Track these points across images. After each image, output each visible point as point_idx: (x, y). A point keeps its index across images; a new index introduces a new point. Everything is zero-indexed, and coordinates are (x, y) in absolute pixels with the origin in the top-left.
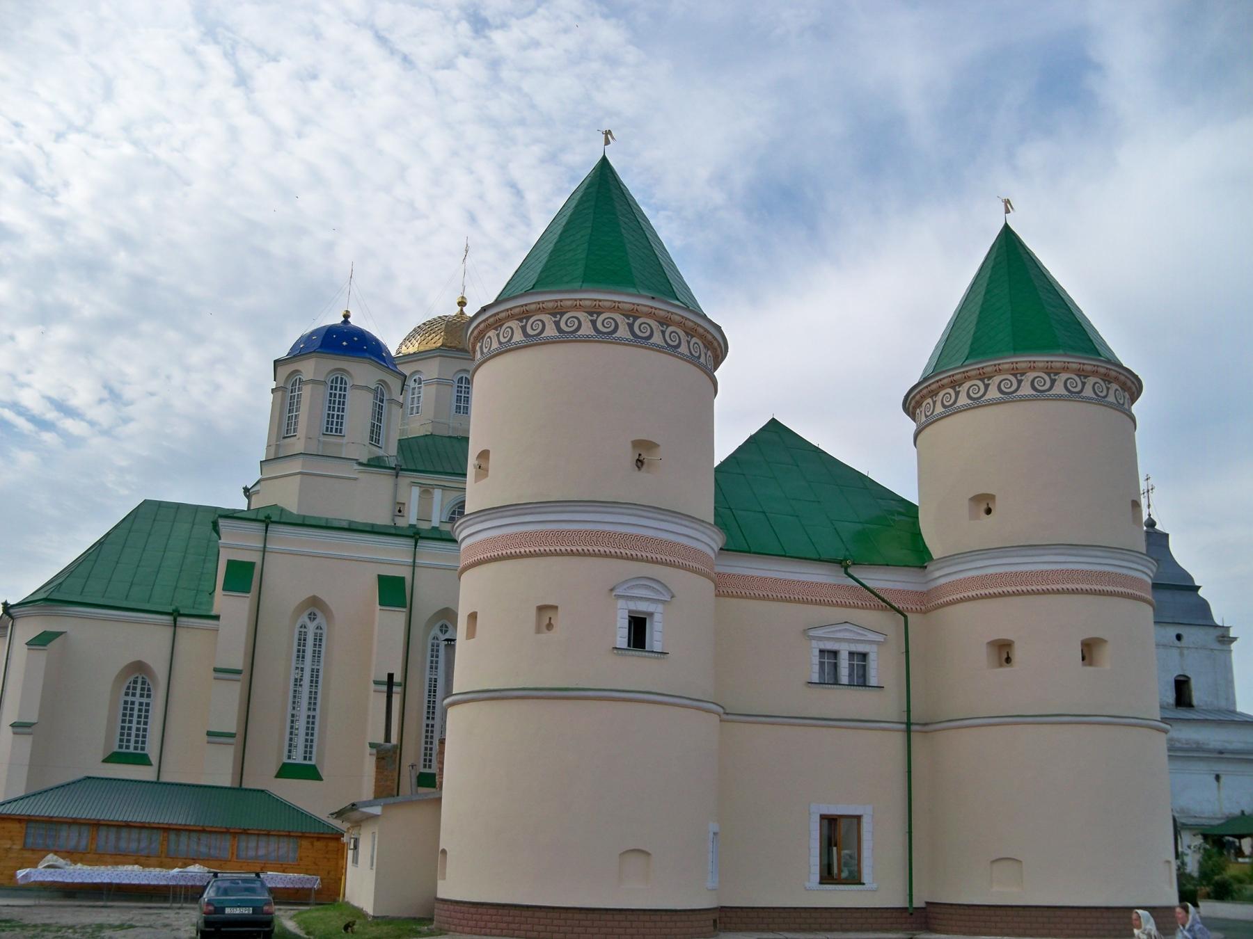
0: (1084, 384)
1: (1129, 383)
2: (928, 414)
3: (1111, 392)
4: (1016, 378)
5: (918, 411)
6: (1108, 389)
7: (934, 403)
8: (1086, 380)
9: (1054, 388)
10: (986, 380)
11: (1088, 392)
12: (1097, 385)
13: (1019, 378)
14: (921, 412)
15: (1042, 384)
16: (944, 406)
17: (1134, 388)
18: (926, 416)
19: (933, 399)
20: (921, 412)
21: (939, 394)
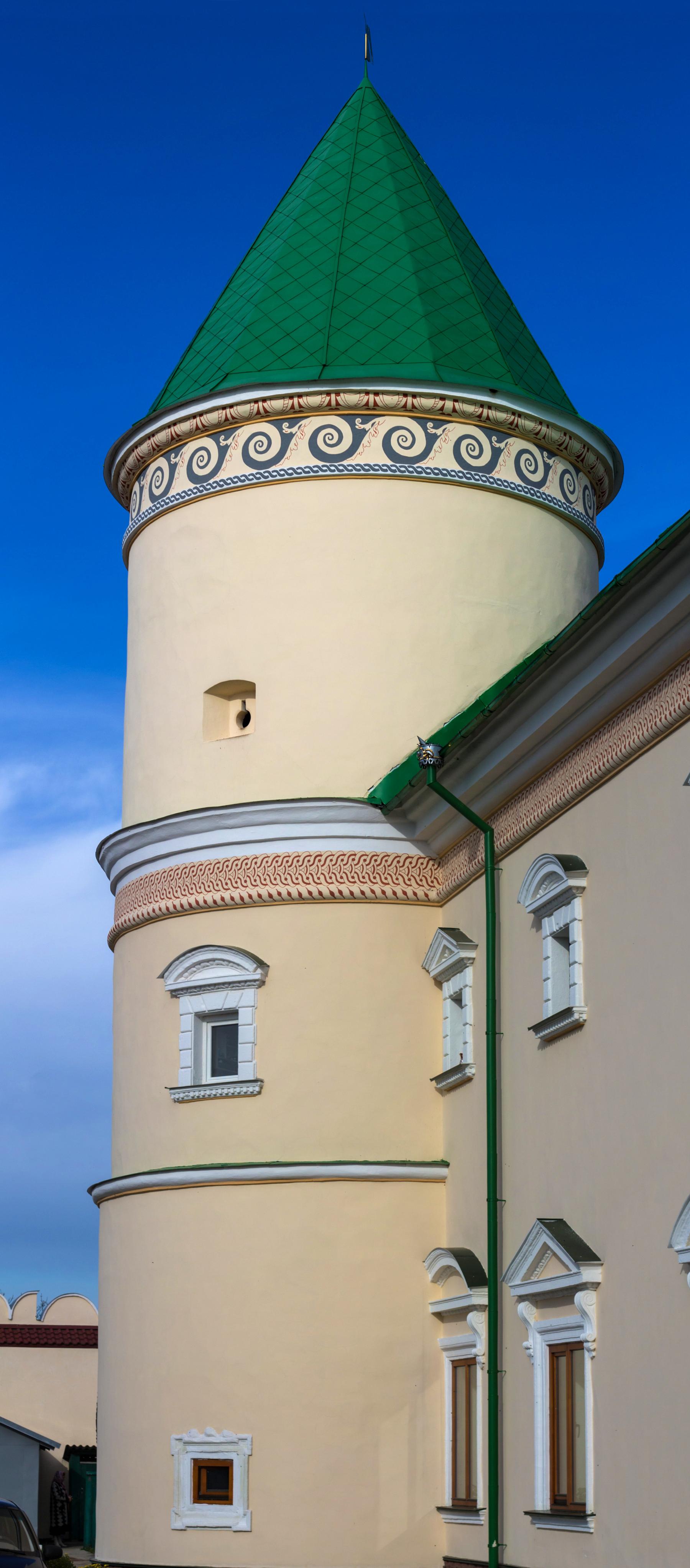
0: (496, 453)
1: (591, 458)
2: (157, 492)
3: (554, 478)
4: (352, 425)
5: (136, 488)
6: (547, 468)
7: (173, 468)
8: (502, 445)
9: (432, 454)
10: (285, 425)
11: (505, 472)
12: (525, 456)
13: (359, 426)
14: (141, 489)
15: (408, 444)
16: (192, 477)
17: (601, 470)
18: (153, 498)
19: (169, 460)
20: (141, 489)
21: (184, 449)
